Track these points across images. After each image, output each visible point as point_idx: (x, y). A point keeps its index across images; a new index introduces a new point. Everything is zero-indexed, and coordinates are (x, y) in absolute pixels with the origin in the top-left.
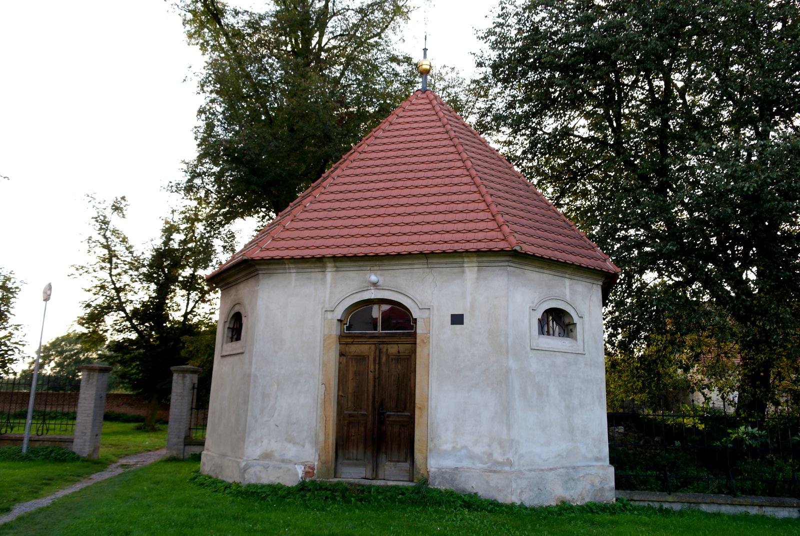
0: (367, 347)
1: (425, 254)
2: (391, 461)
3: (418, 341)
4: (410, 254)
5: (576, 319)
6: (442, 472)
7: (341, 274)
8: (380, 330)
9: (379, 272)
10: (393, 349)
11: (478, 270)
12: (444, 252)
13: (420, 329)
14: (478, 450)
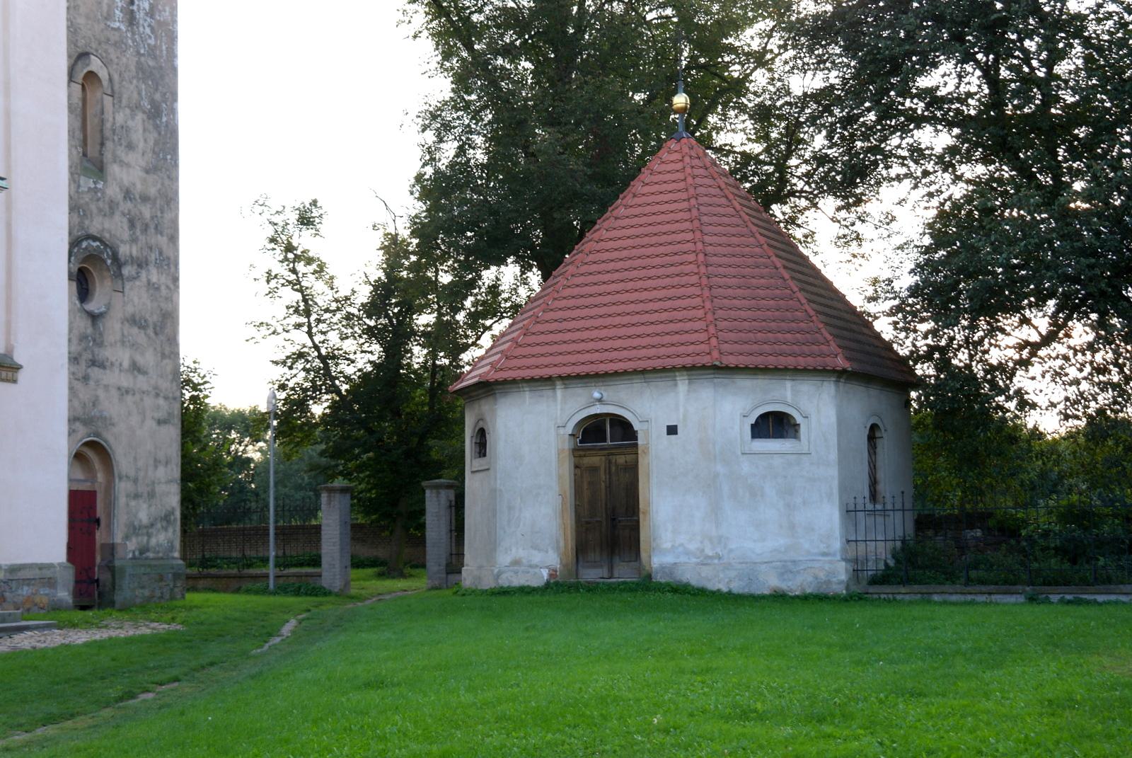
0: (598, 458)
5: (799, 419)
6: (662, 567)
7: (570, 391)
9: (603, 388)
10: (621, 460)
11: (689, 383)
14: (692, 547)
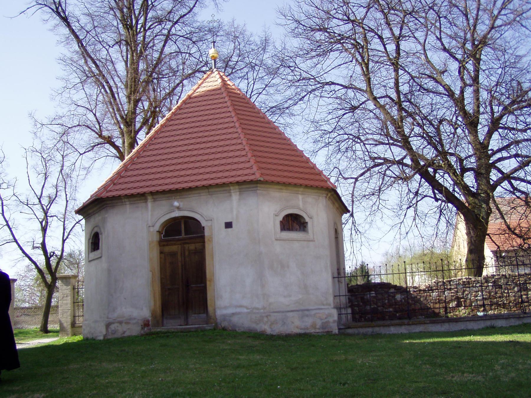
0: (176, 246)
1: (206, 186)
2: (195, 314)
3: (206, 240)
4: (197, 187)
5: (307, 219)
6: (224, 316)
7: (157, 203)
8: (183, 236)
9: (180, 200)
10: (192, 247)
11: (240, 194)
12: (217, 184)
13: (207, 233)
14: (245, 303)
